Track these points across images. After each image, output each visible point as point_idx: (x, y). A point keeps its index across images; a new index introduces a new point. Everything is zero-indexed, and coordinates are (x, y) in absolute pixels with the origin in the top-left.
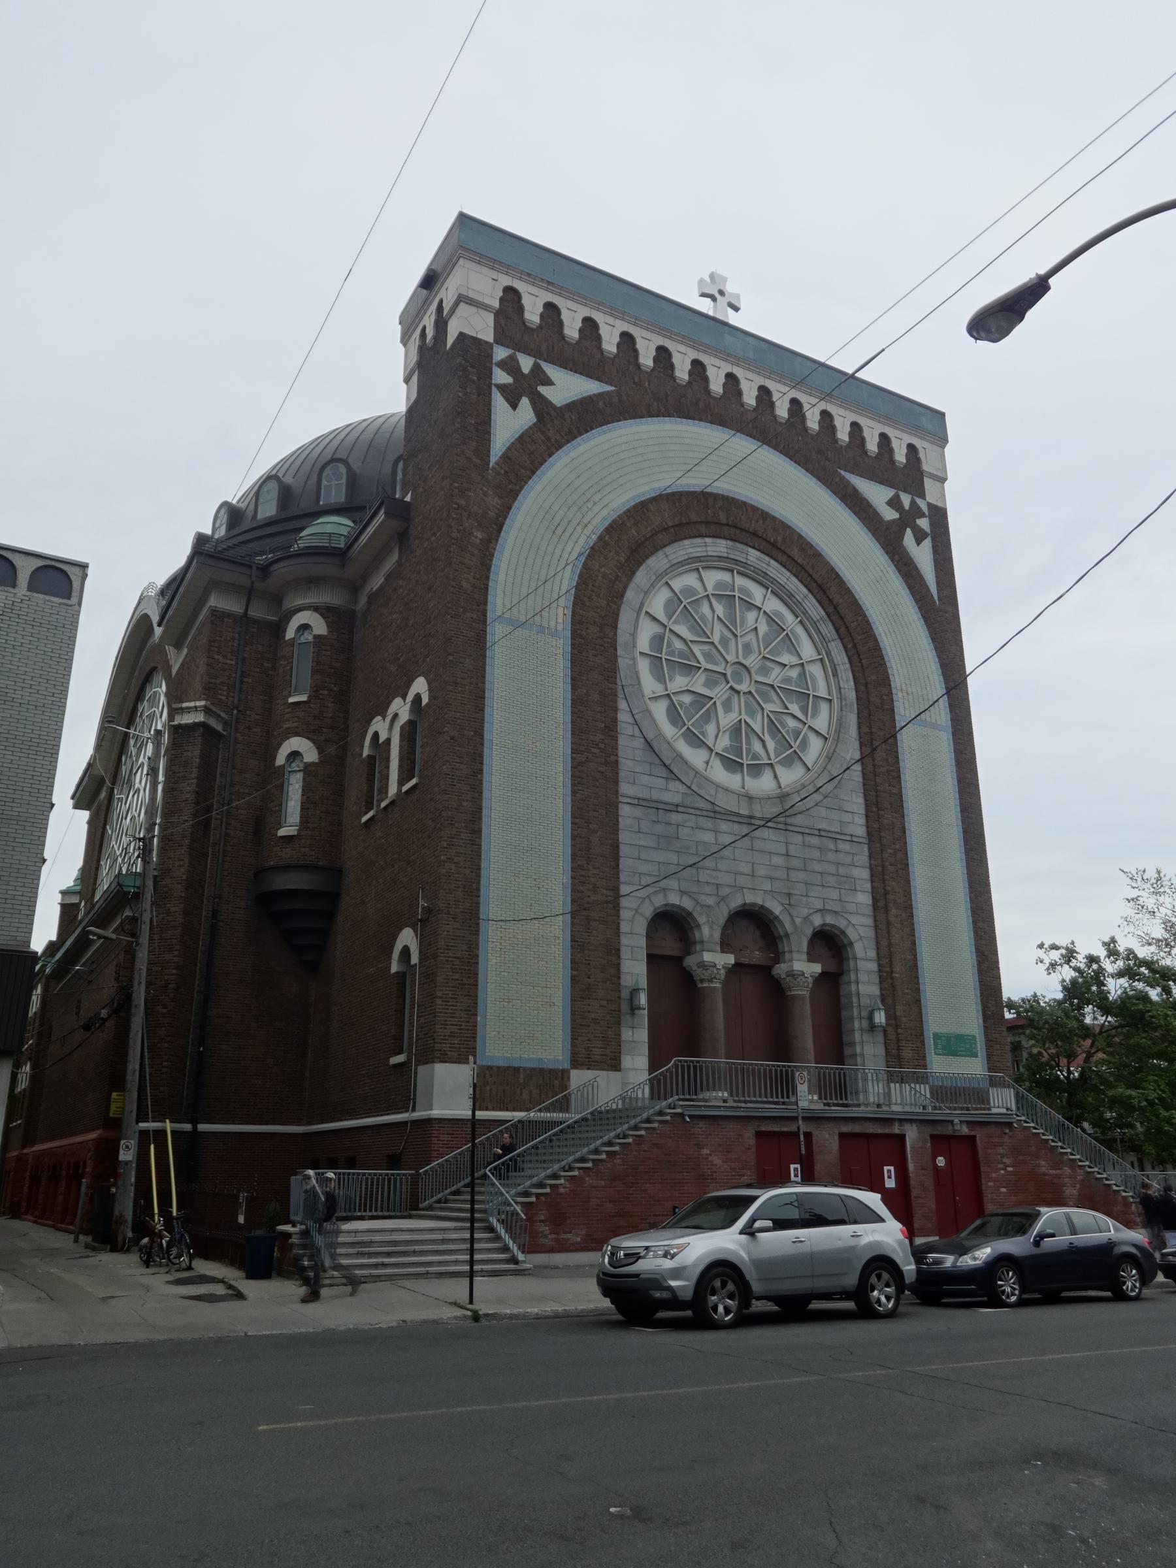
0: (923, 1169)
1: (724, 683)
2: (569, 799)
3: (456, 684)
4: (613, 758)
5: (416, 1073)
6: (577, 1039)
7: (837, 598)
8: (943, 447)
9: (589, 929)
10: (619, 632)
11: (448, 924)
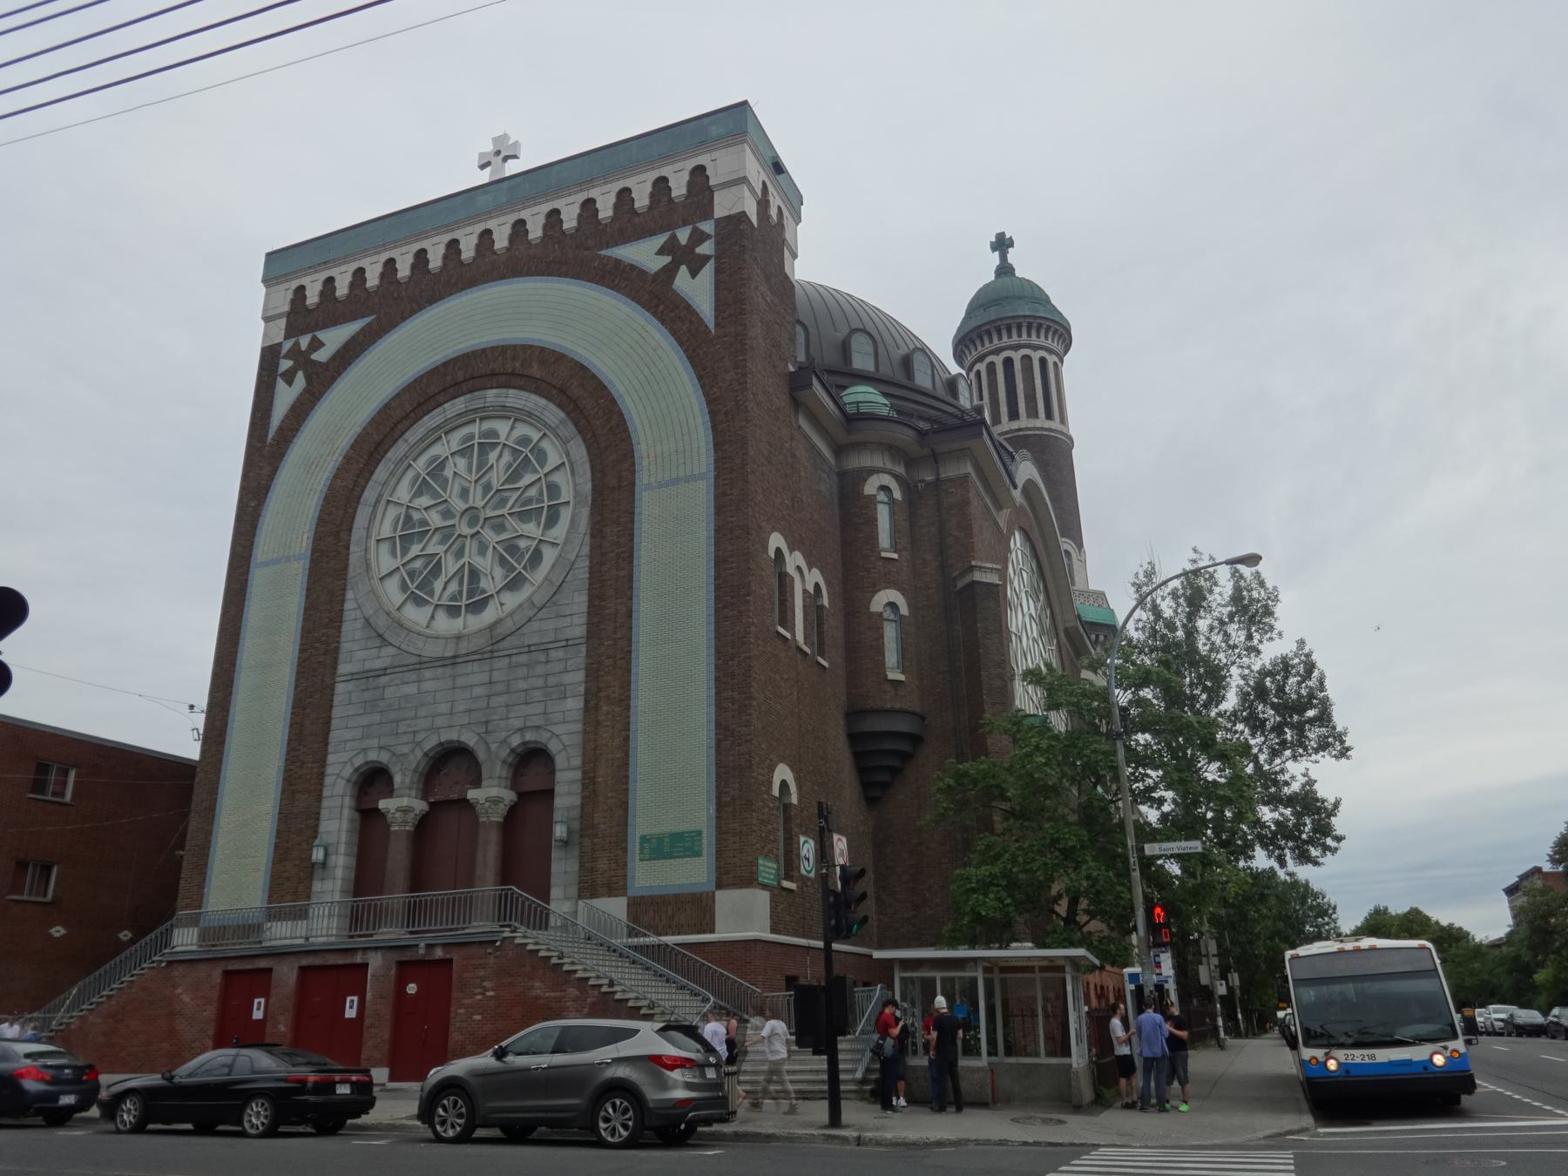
0: (382, 998)
10: (354, 531)
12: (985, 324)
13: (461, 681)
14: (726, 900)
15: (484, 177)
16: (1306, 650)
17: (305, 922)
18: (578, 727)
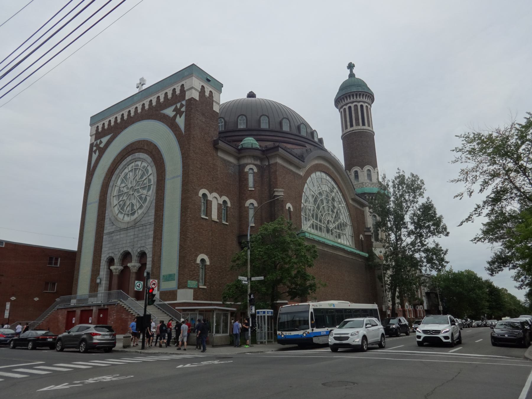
12: (342, 96)
13: (128, 234)
14: (180, 292)
15: (137, 91)
16: (430, 201)
17: (96, 298)
18: (151, 246)
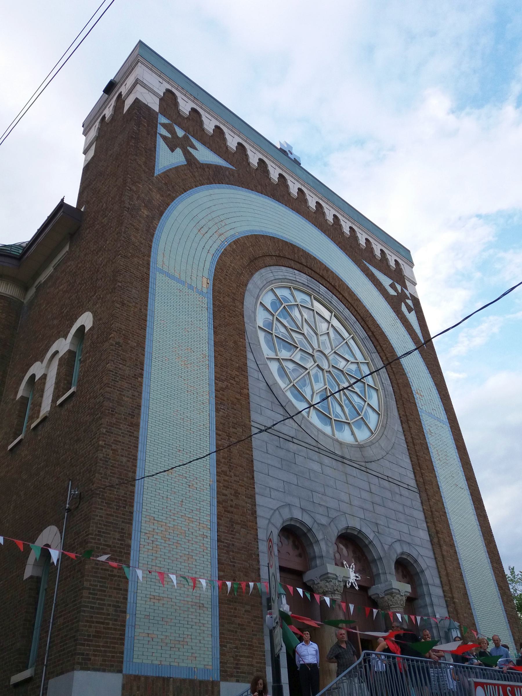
1: (313, 363)
2: (214, 414)
3: (123, 304)
4: (245, 391)
5: (46, 689)
6: (226, 646)
7: (373, 328)
8: (412, 268)
9: (232, 531)
11: (101, 509)
